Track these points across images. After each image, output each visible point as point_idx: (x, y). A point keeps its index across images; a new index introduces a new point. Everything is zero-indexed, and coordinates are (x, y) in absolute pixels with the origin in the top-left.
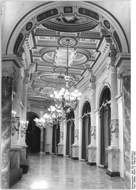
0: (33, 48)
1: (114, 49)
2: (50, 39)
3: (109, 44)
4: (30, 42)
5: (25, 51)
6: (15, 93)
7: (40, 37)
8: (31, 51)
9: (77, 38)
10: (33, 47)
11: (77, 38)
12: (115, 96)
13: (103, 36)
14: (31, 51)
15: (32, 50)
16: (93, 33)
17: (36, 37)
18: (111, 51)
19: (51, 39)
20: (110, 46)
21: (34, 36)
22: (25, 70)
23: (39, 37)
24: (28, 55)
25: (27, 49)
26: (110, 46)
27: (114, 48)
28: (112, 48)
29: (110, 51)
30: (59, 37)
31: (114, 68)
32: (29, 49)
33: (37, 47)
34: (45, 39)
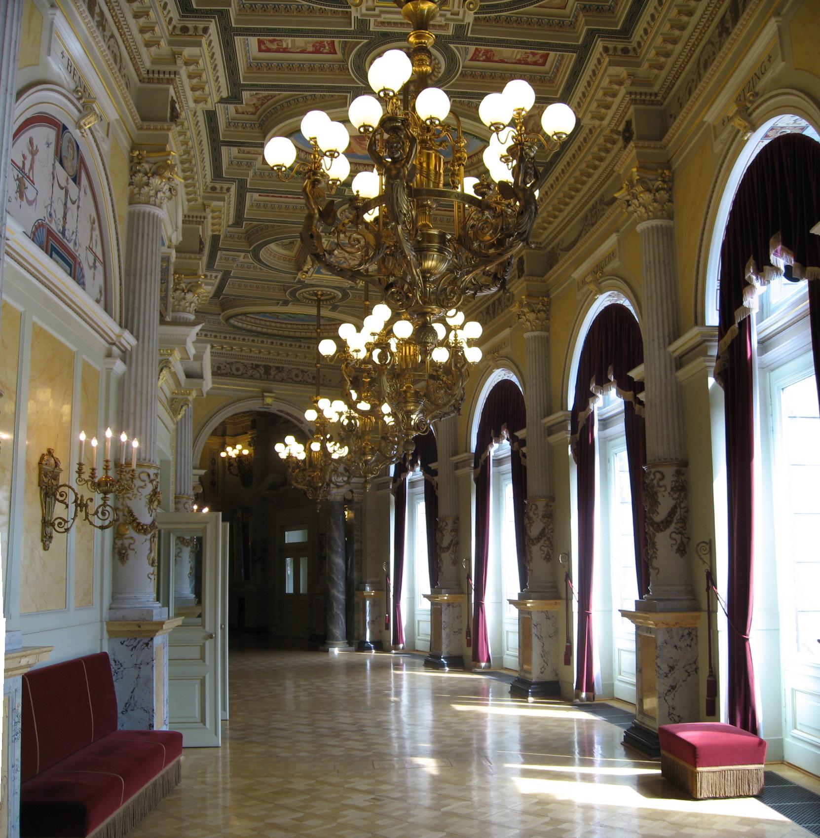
0: (222, 101)
1: (653, 98)
2: (311, 49)
3: (622, 71)
4: (210, 71)
5: (183, 114)
7: (260, 42)
8: (211, 117)
9: (452, 46)
10: (225, 95)
11: (452, 46)
14: (211, 117)
15: (220, 109)
16: (535, 18)
19: (317, 51)
20: (632, 84)
21: (227, 35)
22: (144, 73)
23: (253, 41)
24: (191, 116)
25: (192, 104)
26: (628, 82)
27: (651, 95)
28: (643, 97)
29: (632, 108)
33: (246, 95)
34: (286, 51)
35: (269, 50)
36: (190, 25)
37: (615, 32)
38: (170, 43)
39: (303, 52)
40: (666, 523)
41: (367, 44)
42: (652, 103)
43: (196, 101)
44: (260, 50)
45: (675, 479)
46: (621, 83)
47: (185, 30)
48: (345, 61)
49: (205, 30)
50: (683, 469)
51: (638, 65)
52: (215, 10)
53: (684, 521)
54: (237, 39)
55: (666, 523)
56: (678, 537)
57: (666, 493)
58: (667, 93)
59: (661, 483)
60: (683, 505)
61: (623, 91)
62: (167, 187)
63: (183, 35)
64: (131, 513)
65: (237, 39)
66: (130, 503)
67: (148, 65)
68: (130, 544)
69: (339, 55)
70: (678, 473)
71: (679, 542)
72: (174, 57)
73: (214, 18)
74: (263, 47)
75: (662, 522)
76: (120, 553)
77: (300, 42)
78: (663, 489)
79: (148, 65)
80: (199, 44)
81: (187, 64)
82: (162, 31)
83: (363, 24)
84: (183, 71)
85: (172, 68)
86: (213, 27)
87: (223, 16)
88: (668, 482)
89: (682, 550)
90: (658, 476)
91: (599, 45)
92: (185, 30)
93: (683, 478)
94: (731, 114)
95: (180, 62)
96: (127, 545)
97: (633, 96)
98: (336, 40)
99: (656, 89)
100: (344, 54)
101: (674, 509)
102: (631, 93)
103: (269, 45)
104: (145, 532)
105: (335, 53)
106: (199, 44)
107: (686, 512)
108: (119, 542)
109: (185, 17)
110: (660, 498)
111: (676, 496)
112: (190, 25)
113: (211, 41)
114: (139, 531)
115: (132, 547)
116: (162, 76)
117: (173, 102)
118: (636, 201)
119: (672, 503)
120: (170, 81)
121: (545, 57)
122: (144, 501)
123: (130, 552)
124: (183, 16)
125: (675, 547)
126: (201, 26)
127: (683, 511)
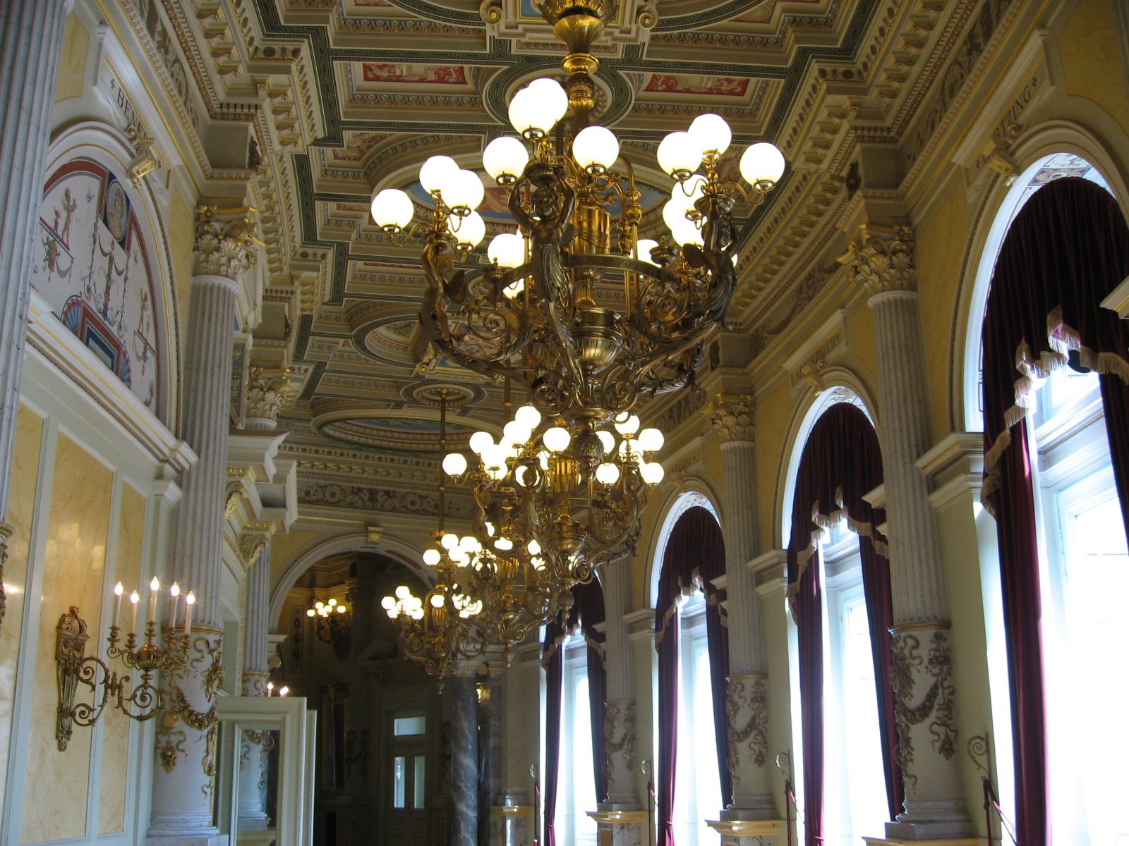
0: (317, 142)
1: (885, 133)
2: (433, 78)
3: (844, 101)
4: (302, 104)
5: (266, 159)
6: (192, 457)
7: (366, 68)
8: (302, 163)
9: (621, 72)
10: (320, 134)
11: (621, 72)
12: (912, 462)
13: (803, 54)
14: (302, 163)
15: (314, 153)
16: (731, 35)
17: (338, 65)
18: (863, 150)
19: (441, 80)
20: (858, 117)
21: (324, 59)
23: (358, 67)
25: (277, 147)
26: (852, 114)
27: (882, 130)
28: (872, 133)
29: (858, 147)
30: (505, 67)
31: (892, 266)
32: (290, 148)
33: (347, 135)
34: (399, 79)
35: (377, 79)
36: (277, 46)
37: (834, 51)
38: (251, 69)
39: (422, 81)
40: (924, 710)
41: (507, 72)
42: (884, 140)
43: (283, 143)
44: (366, 79)
45: (934, 646)
46: (843, 116)
47: (269, 52)
48: (477, 92)
49: (296, 53)
50: (945, 632)
51: (865, 92)
52: (309, 28)
53: (949, 706)
54: (337, 64)
55: (924, 710)
56: (941, 730)
57: (922, 668)
58: (903, 128)
59: (915, 653)
60: (946, 684)
61: (846, 125)
62: (243, 253)
63: (267, 59)
64: (181, 697)
65: (337, 64)
66: (181, 684)
67: (222, 96)
68: (180, 742)
69: (470, 86)
70: (938, 638)
71: (943, 737)
72: (255, 86)
73: (307, 37)
74: (370, 75)
75: (918, 709)
76: (164, 756)
77: (419, 68)
78: (918, 661)
79: (222, 96)
80: (287, 71)
81: (272, 95)
82: (240, 53)
83: (501, 46)
84: (267, 105)
85: (253, 101)
86: (305, 49)
87: (318, 35)
88: (925, 651)
89: (948, 749)
90: (910, 642)
91: (814, 68)
92: (269, 52)
93: (945, 645)
94: (987, 153)
95: (262, 93)
96: (174, 745)
97: (859, 132)
98: (466, 67)
99: (888, 122)
100: (476, 84)
101: (934, 690)
102: (856, 129)
103: (378, 72)
104: (200, 727)
105: (465, 83)
106: (287, 71)
107: (952, 693)
108: (163, 739)
109: (270, 36)
110: (915, 675)
111: (936, 670)
112: (277, 46)
113: (303, 67)
114: (192, 723)
115: (181, 746)
116: (239, 110)
117: (253, 144)
118: (866, 268)
119: (932, 680)
120: (250, 117)
121: (744, 85)
122: (200, 680)
123: (179, 755)
124: (267, 35)
125: (938, 745)
126: (290, 47)
127: (947, 692)
